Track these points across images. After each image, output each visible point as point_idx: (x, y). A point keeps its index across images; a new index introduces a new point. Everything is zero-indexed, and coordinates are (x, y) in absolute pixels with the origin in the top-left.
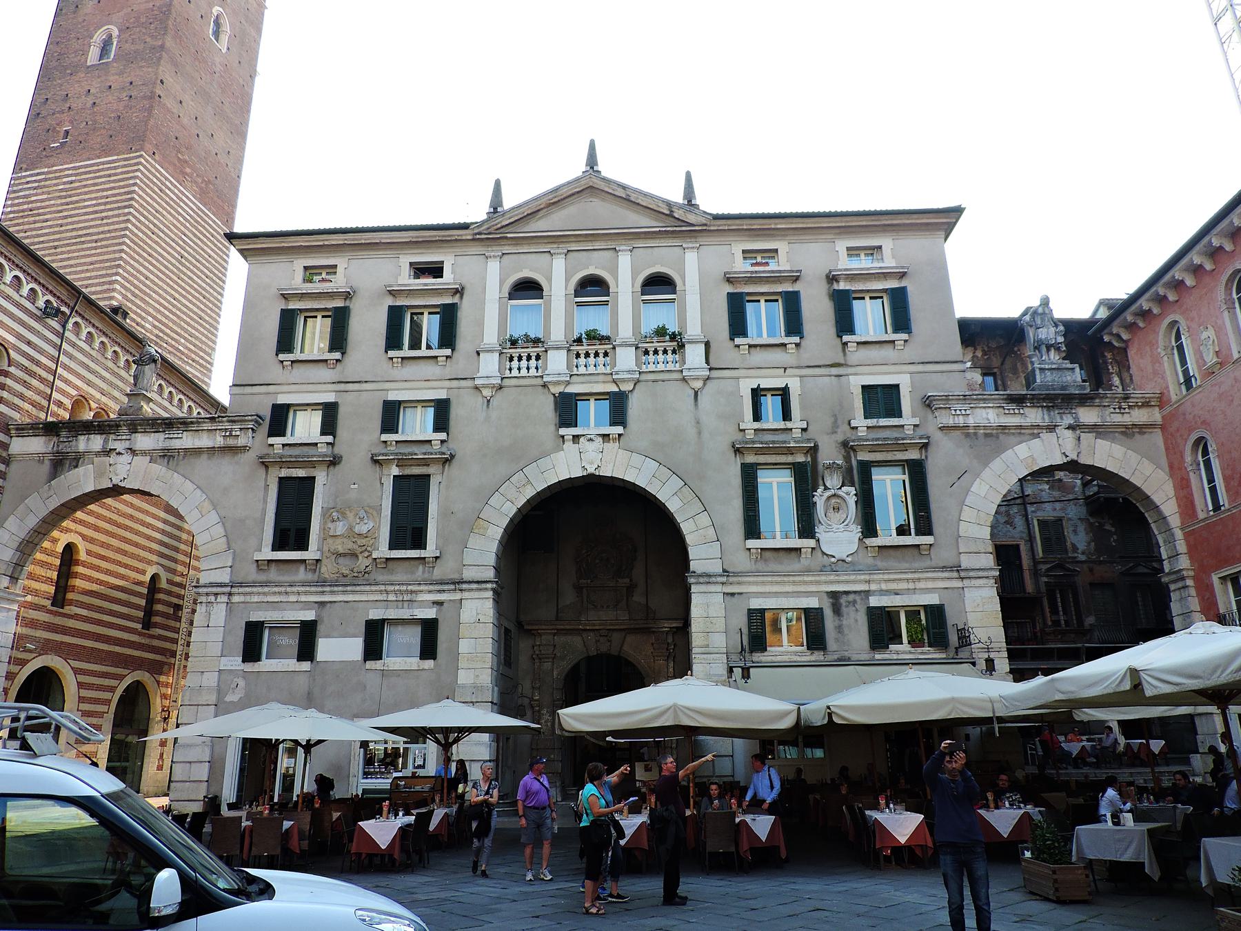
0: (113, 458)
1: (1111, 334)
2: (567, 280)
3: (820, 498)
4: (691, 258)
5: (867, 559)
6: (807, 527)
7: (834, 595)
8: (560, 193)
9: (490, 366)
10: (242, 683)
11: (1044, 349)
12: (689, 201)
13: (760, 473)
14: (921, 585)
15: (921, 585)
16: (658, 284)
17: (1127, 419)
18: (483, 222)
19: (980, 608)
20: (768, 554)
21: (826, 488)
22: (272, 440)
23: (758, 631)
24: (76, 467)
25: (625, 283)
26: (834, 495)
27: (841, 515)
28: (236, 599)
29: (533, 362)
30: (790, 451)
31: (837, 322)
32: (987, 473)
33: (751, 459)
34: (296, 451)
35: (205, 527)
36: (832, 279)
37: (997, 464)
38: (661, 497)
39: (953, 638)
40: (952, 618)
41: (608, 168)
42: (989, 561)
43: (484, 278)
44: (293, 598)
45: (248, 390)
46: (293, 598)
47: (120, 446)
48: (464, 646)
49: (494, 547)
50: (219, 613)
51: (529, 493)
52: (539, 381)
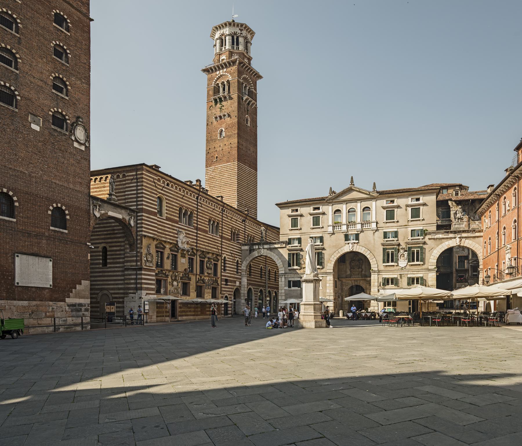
6: (397, 262)
7: (401, 275)
9: (330, 229)
19: (432, 277)
32: (438, 248)
37: (440, 246)
47: (261, 247)
48: (328, 285)
49: (333, 266)
50: (283, 279)
51: (339, 255)
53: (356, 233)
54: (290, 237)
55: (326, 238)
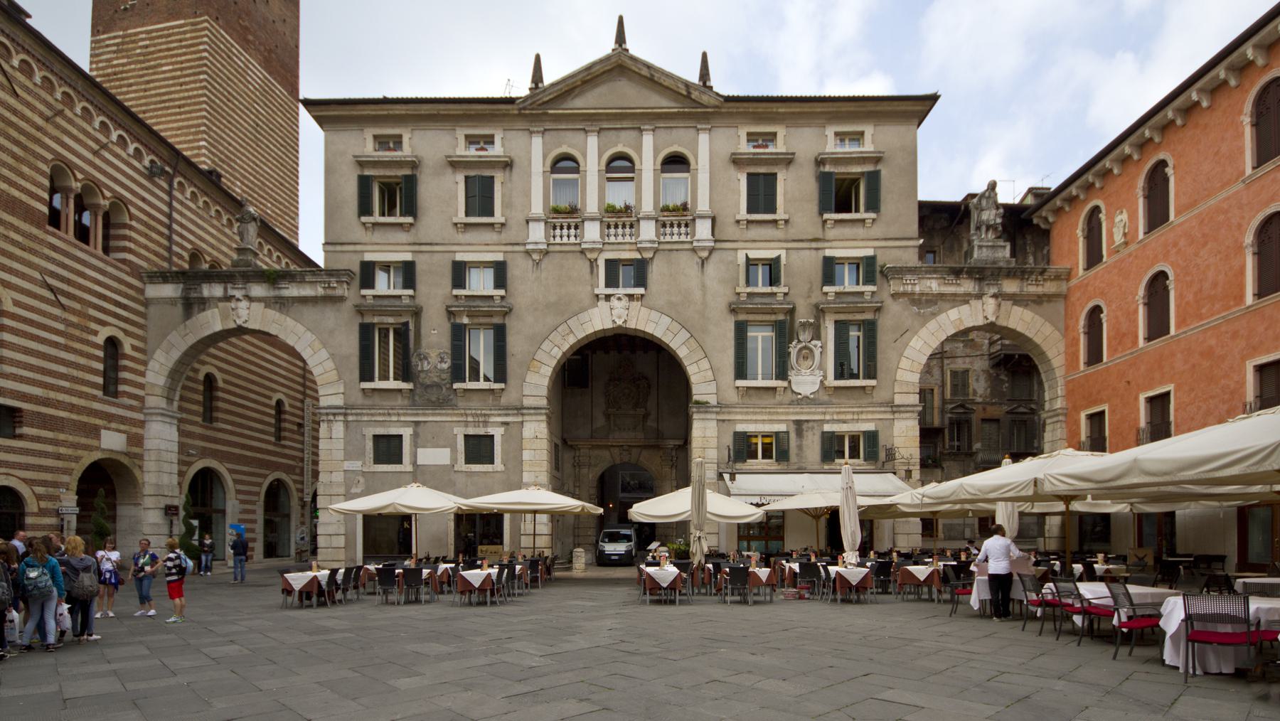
0: (233, 305)
1: (1040, 217)
2: (600, 157)
3: (794, 349)
4: (704, 138)
5: (824, 397)
6: (782, 373)
7: (798, 423)
8: (593, 70)
9: (537, 233)
10: (362, 480)
11: (984, 228)
12: (704, 83)
13: (749, 328)
14: (864, 416)
15: (864, 416)
16: (676, 162)
17: (1040, 290)
18: (526, 98)
19: (904, 436)
20: (751, 392)
21: (799, 341)
22: (364, 292)
23: (742, 449)
24: (204, 310)
25: (648, 162)
26: (805, 348)
27: (809, 362)
28: (350, 418)
29: (572, 231)
30: (773, 312)
31: (820, 201)
32: (923, 332)
33: (742, 317)
34: (386, 302)
35: (320, 363)
36: (820, 162)
37: (932, 325)
38: (673, 345)
39: (882, 455)
40: (882, 440)
41: (635, 48)
42: (914, 399)
43: (529, 152)
44: (395, 418)
45: (339, 248)
46: (395, 418)
47: (238, 294)
48: (526, 455)
49: (545, 382)
50: (339, 429)
51: (572, 340)
52: (577, 248)
53: (637, 256)
54: (369, 257)
55: (519, 269)
